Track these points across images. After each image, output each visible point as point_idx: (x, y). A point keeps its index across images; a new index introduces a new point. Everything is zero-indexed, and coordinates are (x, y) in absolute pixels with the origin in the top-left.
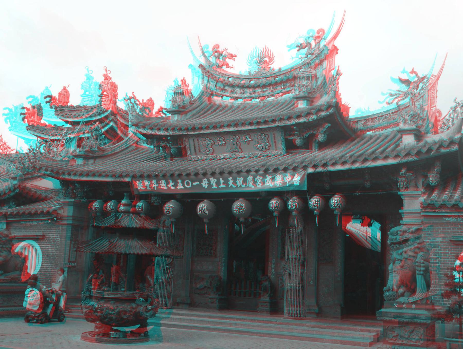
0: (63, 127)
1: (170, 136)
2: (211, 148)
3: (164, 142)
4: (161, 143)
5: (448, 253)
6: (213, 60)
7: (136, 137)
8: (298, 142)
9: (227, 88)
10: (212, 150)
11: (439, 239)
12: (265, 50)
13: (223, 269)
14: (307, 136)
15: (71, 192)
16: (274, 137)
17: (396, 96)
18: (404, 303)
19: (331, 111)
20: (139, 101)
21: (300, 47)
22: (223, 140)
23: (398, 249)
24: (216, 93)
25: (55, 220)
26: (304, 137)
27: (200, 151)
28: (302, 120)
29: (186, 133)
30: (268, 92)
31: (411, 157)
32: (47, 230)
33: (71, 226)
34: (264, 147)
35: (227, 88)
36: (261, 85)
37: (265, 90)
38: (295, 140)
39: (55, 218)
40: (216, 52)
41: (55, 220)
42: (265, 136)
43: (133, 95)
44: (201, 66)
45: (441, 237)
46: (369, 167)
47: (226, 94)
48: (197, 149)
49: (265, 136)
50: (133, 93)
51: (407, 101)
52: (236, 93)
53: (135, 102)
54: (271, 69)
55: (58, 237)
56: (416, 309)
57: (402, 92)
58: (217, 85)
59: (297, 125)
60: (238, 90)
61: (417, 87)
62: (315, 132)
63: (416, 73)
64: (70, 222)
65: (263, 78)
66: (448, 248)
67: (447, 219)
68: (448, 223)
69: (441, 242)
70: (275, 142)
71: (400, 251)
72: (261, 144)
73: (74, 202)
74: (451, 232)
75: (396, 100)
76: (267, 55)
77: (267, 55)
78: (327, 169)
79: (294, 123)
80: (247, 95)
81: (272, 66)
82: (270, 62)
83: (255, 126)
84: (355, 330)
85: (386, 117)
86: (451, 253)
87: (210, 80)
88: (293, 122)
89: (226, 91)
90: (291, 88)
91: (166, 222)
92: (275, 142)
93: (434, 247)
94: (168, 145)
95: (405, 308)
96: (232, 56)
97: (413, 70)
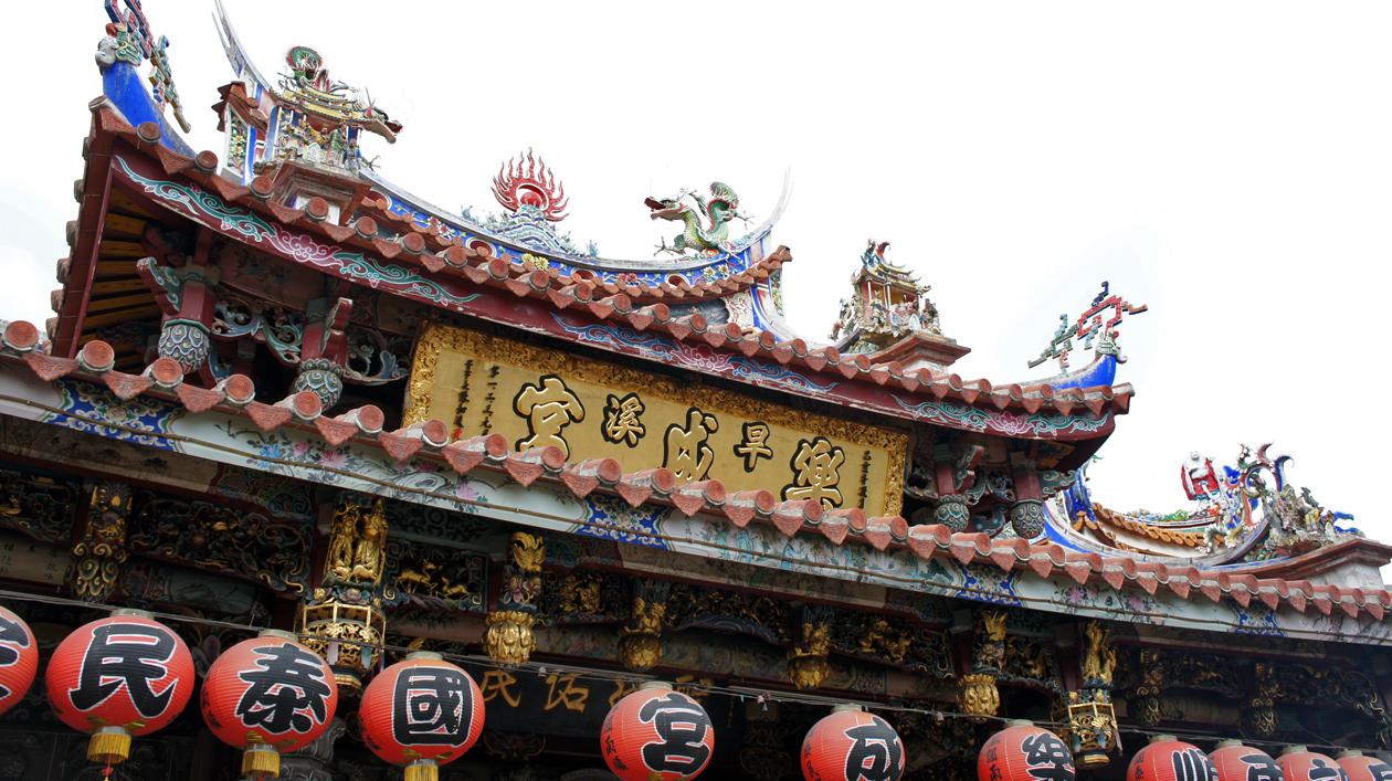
2: (559, 435)
3: (247, 322)
4: (221, 316)
16: (865, 466)
22: (638, 414)
28: (1011, 428)
42: (832, 454)
62: (1003, 493)
65: (538, 255)
70: (863, 492)
72: (808, 484)
83: (835, 390)
94: (280, 348)
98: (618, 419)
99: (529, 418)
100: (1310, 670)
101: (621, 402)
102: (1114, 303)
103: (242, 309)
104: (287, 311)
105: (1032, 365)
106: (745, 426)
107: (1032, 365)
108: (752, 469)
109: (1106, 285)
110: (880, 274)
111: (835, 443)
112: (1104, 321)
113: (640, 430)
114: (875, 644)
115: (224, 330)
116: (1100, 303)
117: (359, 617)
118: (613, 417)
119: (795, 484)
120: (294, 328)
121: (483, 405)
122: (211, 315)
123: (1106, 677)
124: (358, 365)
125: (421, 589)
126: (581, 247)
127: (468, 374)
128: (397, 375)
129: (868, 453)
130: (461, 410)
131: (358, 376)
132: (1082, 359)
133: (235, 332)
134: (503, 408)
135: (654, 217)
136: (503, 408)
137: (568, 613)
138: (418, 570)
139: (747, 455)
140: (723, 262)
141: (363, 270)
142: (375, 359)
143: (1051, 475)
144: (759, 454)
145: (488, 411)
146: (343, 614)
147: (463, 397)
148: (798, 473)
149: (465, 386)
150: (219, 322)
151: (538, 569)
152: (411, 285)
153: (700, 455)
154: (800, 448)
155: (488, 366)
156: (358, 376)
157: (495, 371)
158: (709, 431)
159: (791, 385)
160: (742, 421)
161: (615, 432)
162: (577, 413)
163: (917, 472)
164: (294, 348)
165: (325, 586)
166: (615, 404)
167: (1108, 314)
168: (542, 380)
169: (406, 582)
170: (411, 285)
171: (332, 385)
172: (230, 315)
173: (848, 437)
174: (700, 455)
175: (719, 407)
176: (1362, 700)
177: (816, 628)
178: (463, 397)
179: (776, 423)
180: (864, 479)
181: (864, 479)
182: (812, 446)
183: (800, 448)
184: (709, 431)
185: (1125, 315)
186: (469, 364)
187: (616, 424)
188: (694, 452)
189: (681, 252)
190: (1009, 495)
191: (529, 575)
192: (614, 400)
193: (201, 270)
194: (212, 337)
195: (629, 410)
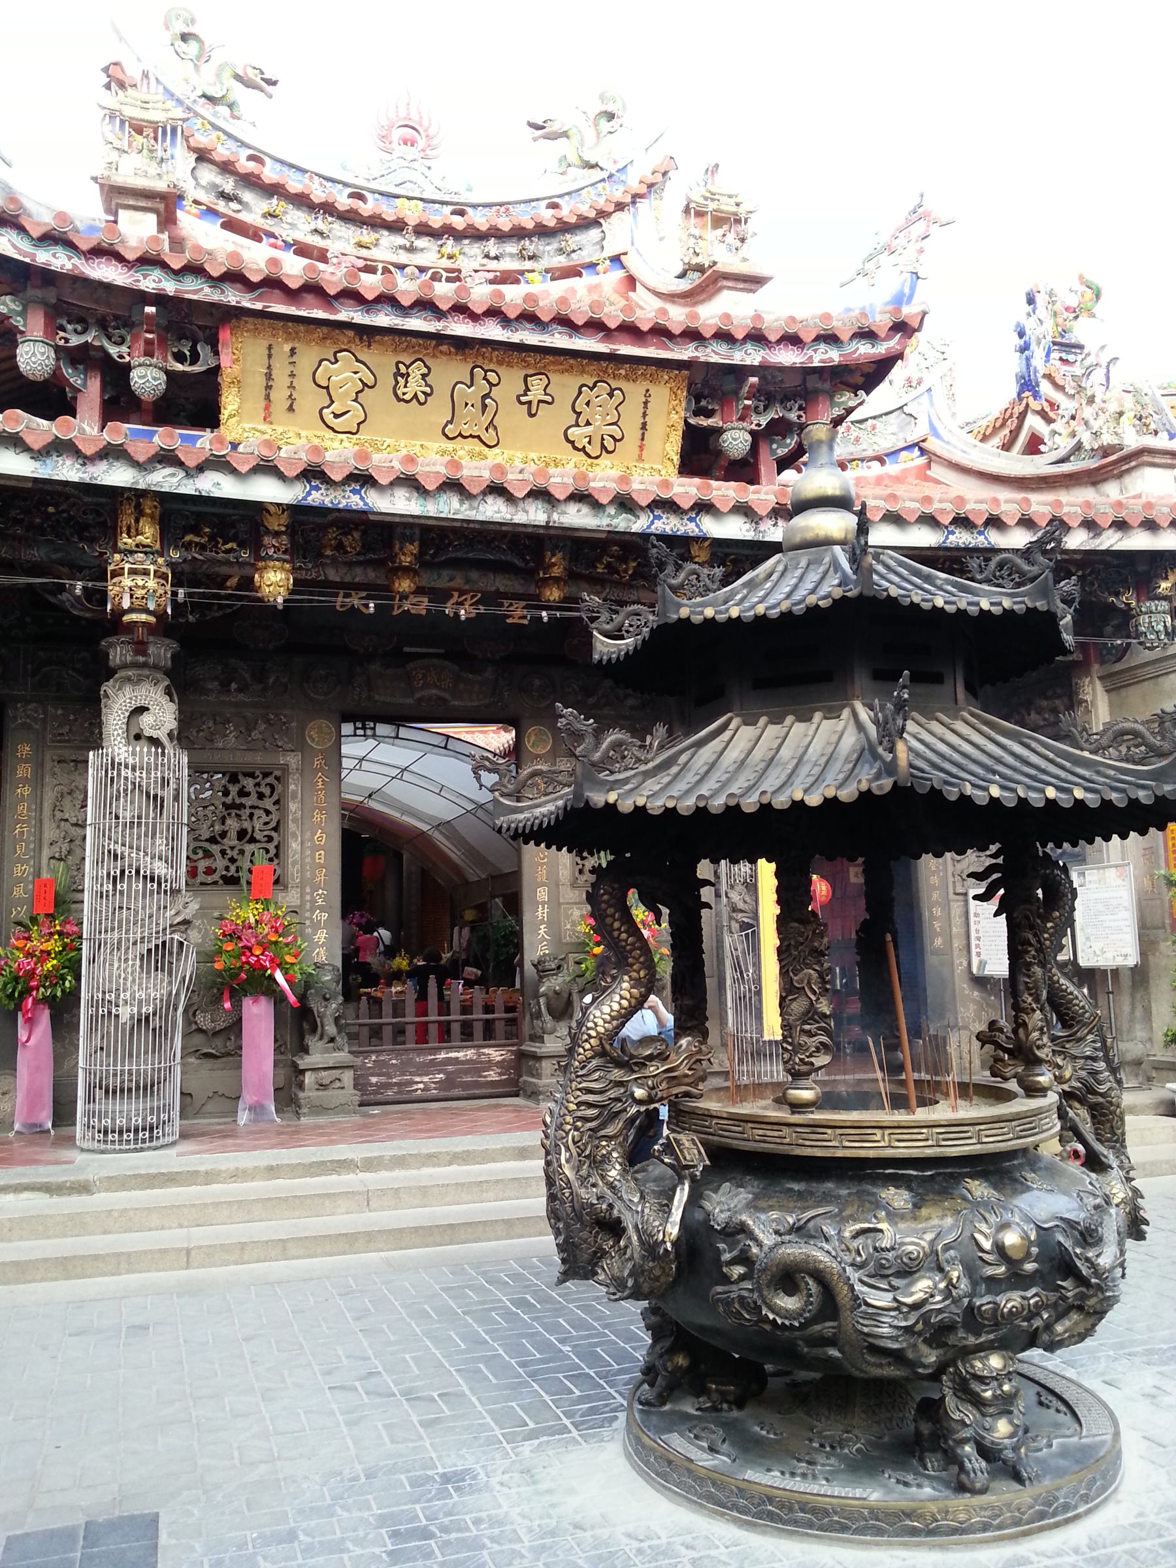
1: (159, 299)
2: (355, 400)
3: (84, 332)
4: (64, 330)
8: (736, 441)
10: (357, 413)
13: (321, 936)
16: (646, 403)
22: (424, 376)
24: (196, 202)
26: (753, 427)
27: (291, 409)
28: (787, 357)
29: (259, 306)
34: (597, 441)
36: (412, 222)
38: (719, 431)
42: (611, 395)
46: (1114, 548)
48: (280, 395)
49: (611, 395)
58: (199, 173)
59: (763, 370)
62: (793, 416)
70: (644, 426)
72: (588, 423)
78: (986, 538)
83: (602, 341)
88: (751, 356)
90: (528, 265)
92: (644, 426)
94: (113, 350)
98: (407, 382)
99: (327, 388)
101: (408, 367)
102: (925, 216)
103: (80, 320)
106: (526, 377)
108: (534, 415)
110: (706, 199)
111: (614, 385)
112: (913, 237)
113: (428, 390)
114: (608, 566)
115: (67, 340)
117: (146, 573)
118: (401, 381)
119: (577, 425)
120: (123, 332)
121: (287, 381)
122: (52, 328)
124: (180, 358)
125: (203, 547)
127: (270, 356)
128: (212, 363)
129: (647, 391)
130: (268, 387)
131: (179, 367)
133: (75, 341)
134: (304, 383)
135: (535, 139)
136: (304, 383)
137: (328, 557)
138: (198, 533)
139: (529, 403)
141: (160, 281)
143: (842, 396)
144: (540, 401)
145: (291, 387)
146: (133, 572)
147: (269, 376)
148: (579, 414)
149: (269, 367)
150: (62, 334)
151: (283, 529)
152: (202, 289)
153: (485, 406)
154: (580, 393)
155: (287, 348)
156: (179, 367)
157: (293, 352)
158: (491, 385)
159: (560, 340)
160: (524, 373)
161: (404, 394)
162: (370, 380)
163: (703, 403)
164: (124, 349)
165: (120, 552)
166: (403, 369)
167: (919, 228)
168: (335, 354)
169: (190, 543)
170: (202, 289)
171: (155, 379)
172: (69, 327)
173: (627, 378)
174: (485, 406)
175: (500, 363)
177: (553, 555)
178: (269, 376)
179: (555, 371)
180: (645, 415)
181: (645, 415)
182: (591, 389)
183: (580, 393)
184: (491, 385)
185: (934, 229)
186: (270, 348)
187: (405, 386)
188: (479, 405)
190: (799, 417)
191: (277, 534)
192: (401, 366)
193: (39, 293)
194: (57, 349)
195: (416, 371)
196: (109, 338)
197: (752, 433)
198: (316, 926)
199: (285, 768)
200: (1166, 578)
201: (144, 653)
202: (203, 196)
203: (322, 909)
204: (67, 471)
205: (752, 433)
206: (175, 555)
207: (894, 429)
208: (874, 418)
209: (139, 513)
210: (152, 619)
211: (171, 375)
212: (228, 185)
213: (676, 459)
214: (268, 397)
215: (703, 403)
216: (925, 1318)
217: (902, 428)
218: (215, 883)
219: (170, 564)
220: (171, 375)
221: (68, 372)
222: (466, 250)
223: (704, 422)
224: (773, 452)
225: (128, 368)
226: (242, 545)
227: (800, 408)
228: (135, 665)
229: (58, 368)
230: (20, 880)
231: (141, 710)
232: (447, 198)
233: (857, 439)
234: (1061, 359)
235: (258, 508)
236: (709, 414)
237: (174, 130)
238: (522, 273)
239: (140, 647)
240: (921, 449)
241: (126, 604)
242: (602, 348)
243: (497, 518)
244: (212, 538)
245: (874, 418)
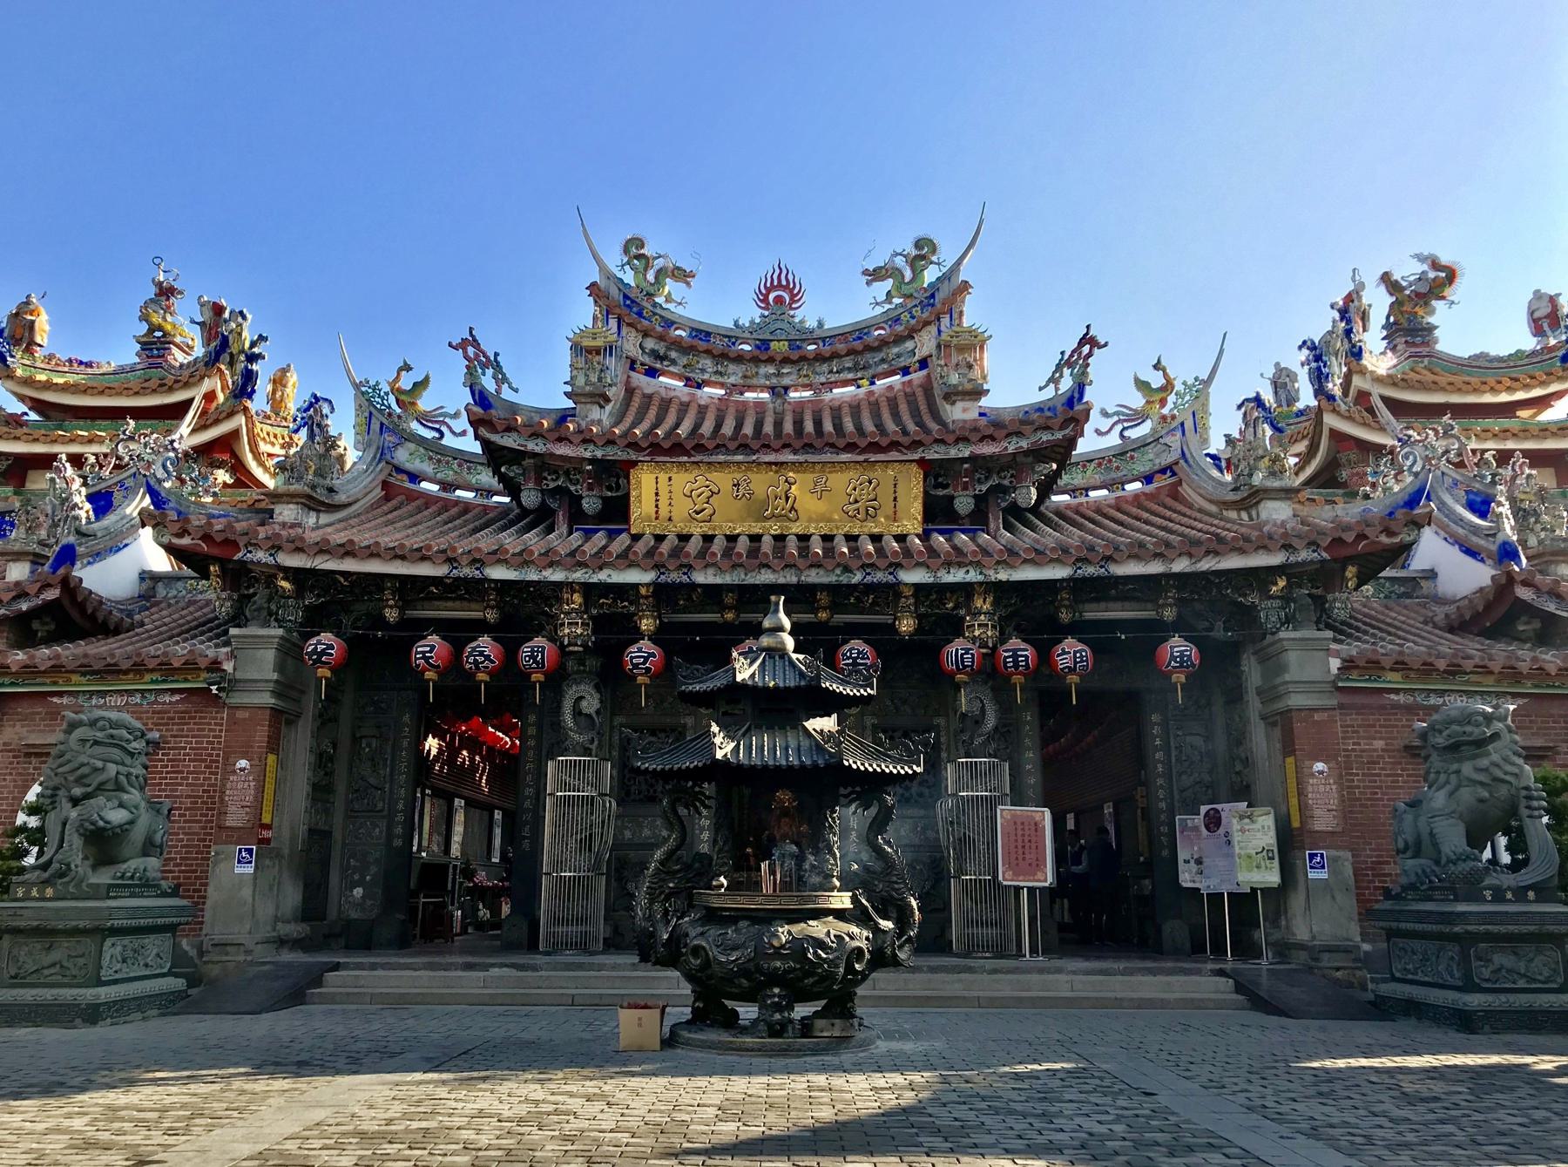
0: (26, 418)
1: (592, 461)
5: (1402, 775)
6: (629, 277)
7: (383, 464)
8: (964, 504)
9: (673, 354)
11: (1379, 744)
12: (777, 271)
13: (706, 835)
14: (984, 488)
15: (266, 605)
17: (1116, 418)
18: (1509, 888)
19: (1067, 431)
20: (485, 355)
21: (875, 275)
23: (1475, 757)
24: (642, 364)
25: (214, 692)
30: (794, 377)
31: (1314, 551)
32: (168, 724)
33: (268, 712)
35: (673, 354)
37: (785, 371)
38: (952, 498)
39: (214, 688)
40: (639, 257)
41: (214, 692)
42: (870, 483)
43: (471, 333)
44: (593, 287)
45: (1381, 739)
47: (672, 369)
50: (471, 329)
51: (1144, 429)
52: (703, 371)
53: (477, 356)
54: (797, 320)
55: (213, 749)
56: (1536, 901)
57: (1130, 409)
59: (973, 459)
60: (707, 363)
61: (1163, 402)
62: (1006, 482)
63: (1164, 370)
64: (267, 699)
66: (1400, 763)
67: (1392, 696)
68: (1396, 706)
69: (1383, 750)
71: (1484, 762)
73: (282, 638)
74: (1403, 726)
75: (1119, 427)
76: (784, 283)
77: (784, 283)
79: (967, 454)
80: (732, 380)
81: (799, 315)
82: (793, 301)
84: (1198, 972)
85: (1100, 465)
86: (1408, 776)
87: (625, 330)
89: (673, 362)
91: (584, 704)
93: (1368, 763)
94: (572, 488)
95: (1510, 901)
96: (682, 275)
97: (1159, 361)
100: (1212, 578)
103: (556, 472)
104: (575, 469)
105: (1041, 389)
107: (1041, 389)
109: (1088, 327)
114: (857, 598)
116: (1082, 343)
122: (539, 480)
123: (987, 607)
124: (610, 488)
126: (811, 323)
131: (609, 494)
132: (1066, 383)
133: (552, 485)
135: (868, 283)
140: (916, 306)
142: (617, 484)
153: (787, 499)
156: (609, 494)
163: (940, 480)
167: (1086, 349)
176: (1245, 595)
178: (657, 494)
189: (891, 303)
191: (646, 597)
194: (542, 491)
196: (571, 480)
197: (975, 497)
198: (702, 829)
199: (684, 726)
200: (1276, 584)
201: (584, 665)
202: (647, 360)
203: (706, 818)
204: (533, 576)
205: (975, 497)
206: (594, 612)
207: (1151, 456)
208: (1133, 450)
209: (573, 591)
210: (581, 649)
211: (605, 500)
212: (661, 348)
213: (920, 518)
214: (657, 506)
215: (940, 480)
216: (738, 966)
217: (1157, 455)
218: (640, 800)
219: (591, 618)
220: (605, 500)
221: (549, 502)
222: (818, 369)
223: (941, 492)
224: (999, 505)
225: (581, 497)
226: (631, 603)
227: (1012, 476)
228: (578, 672)
229: (543, 500)
230: (529, 797)
231: (582, 698)
232: (804, 337)
233: (1118, 468)
234: (1406, 342)
235: (635, 586)
236: (945, 486)
237: (611, 347)
238: (856, 380)
239: (581, 662)
240: (1172, 471)
241: (566, 643)
242: (861, 458)
243: (767, 582)
244: (615, 600)
245: (1133, 450)
